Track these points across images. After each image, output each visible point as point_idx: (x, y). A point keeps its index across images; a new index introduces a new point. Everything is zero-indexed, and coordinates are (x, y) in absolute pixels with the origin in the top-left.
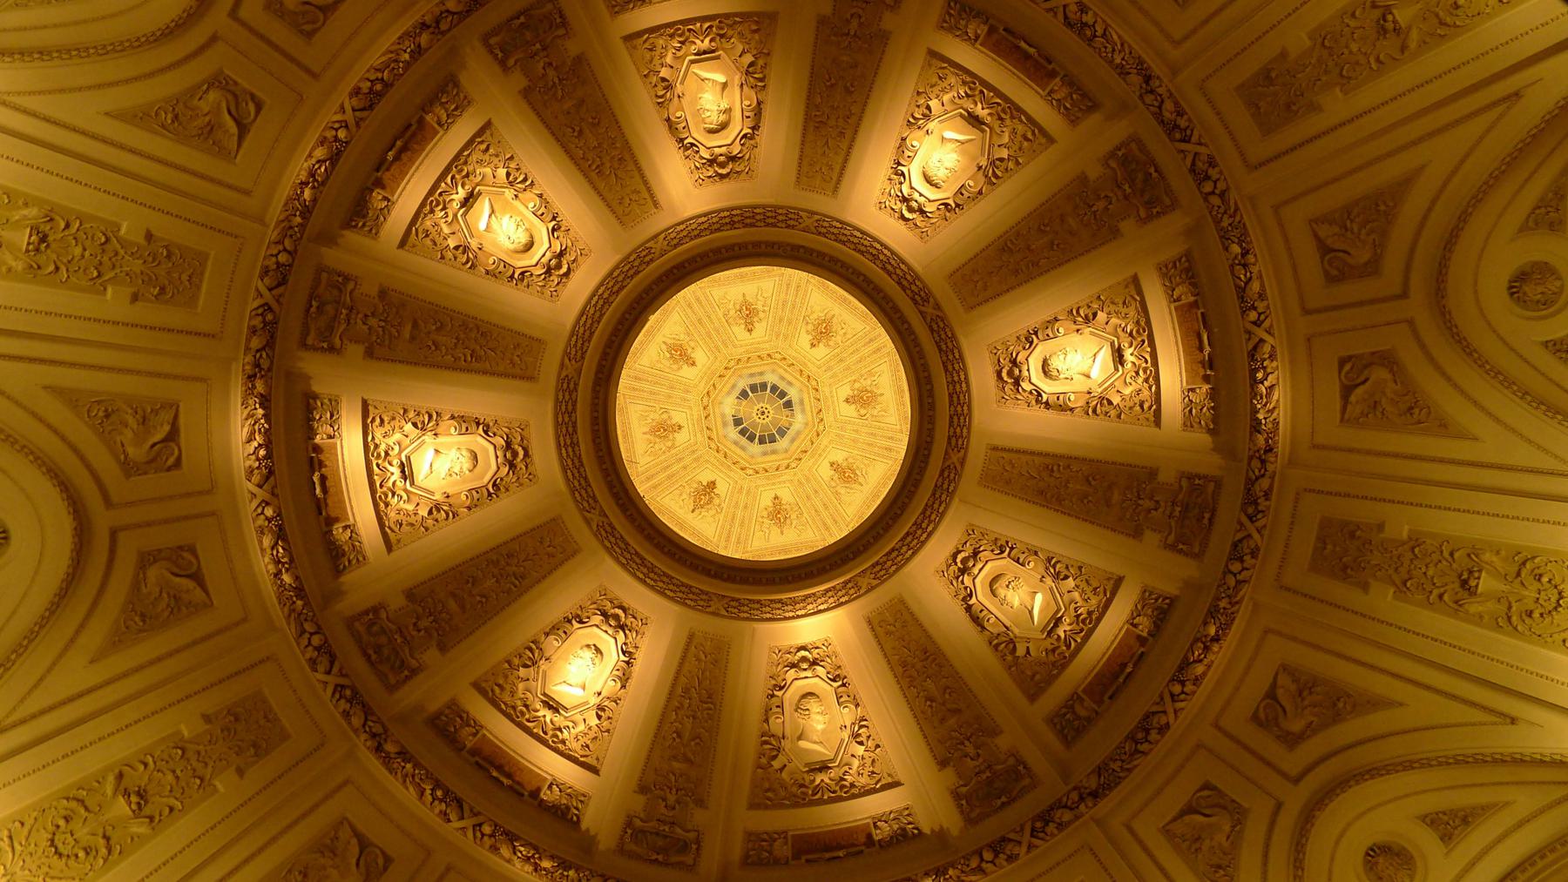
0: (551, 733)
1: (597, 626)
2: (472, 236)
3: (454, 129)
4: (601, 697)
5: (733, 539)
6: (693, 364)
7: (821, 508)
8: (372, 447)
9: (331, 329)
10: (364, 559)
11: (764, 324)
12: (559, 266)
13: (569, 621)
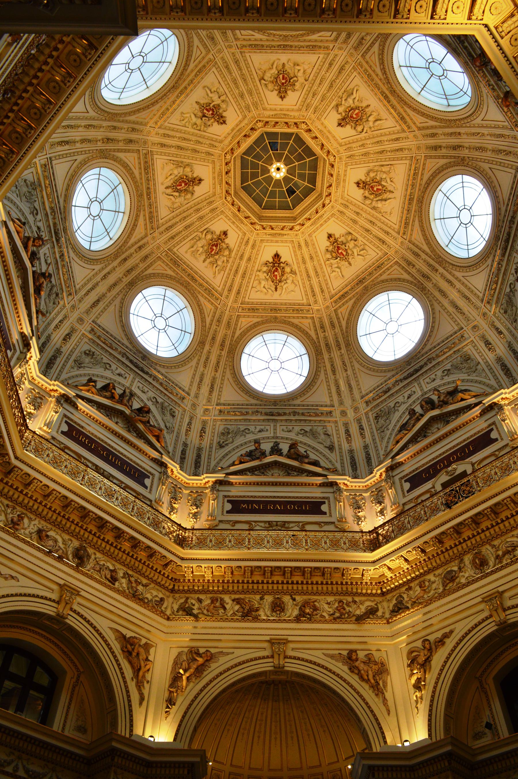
5: (317, 290)
6: (200, 180)
7: (369, 226)
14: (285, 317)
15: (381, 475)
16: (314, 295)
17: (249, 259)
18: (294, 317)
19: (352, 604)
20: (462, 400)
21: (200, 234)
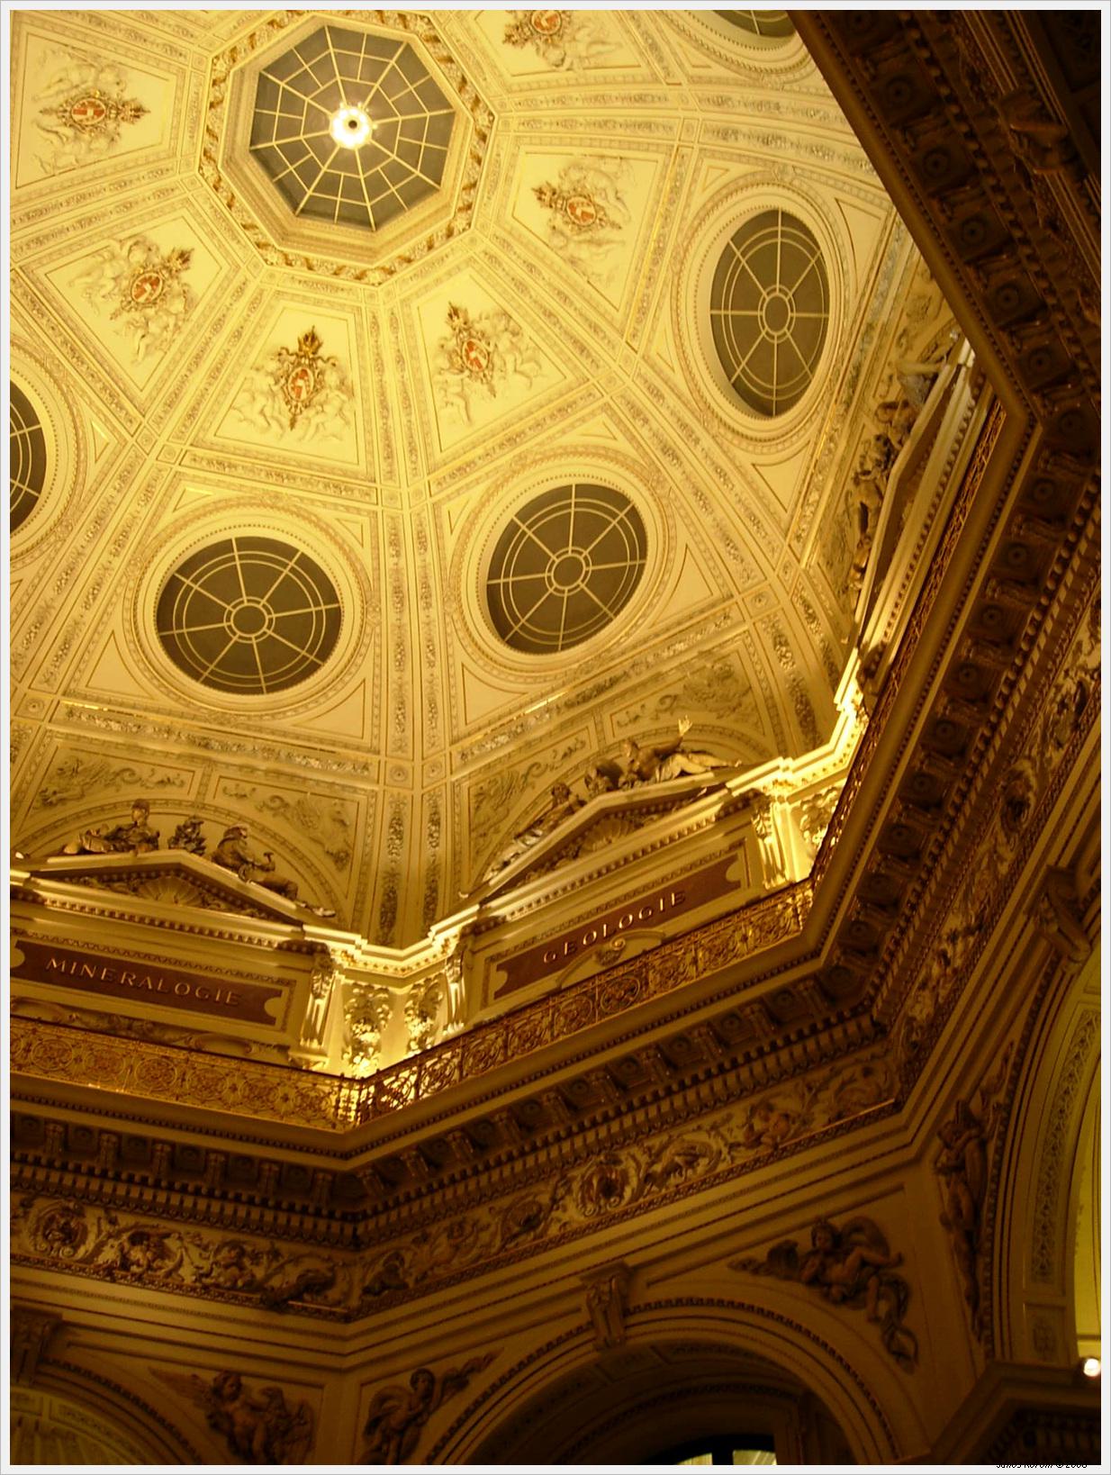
5: (399, 444)
6: (138, 112)
7: (554, 305)
14: (301, 499)
15: (445, 946)
16: (389, 456)
17: (238, 334)
18: (324, 504)
19: (265, 1260)
20: (683, 774)
21: (117, 246)
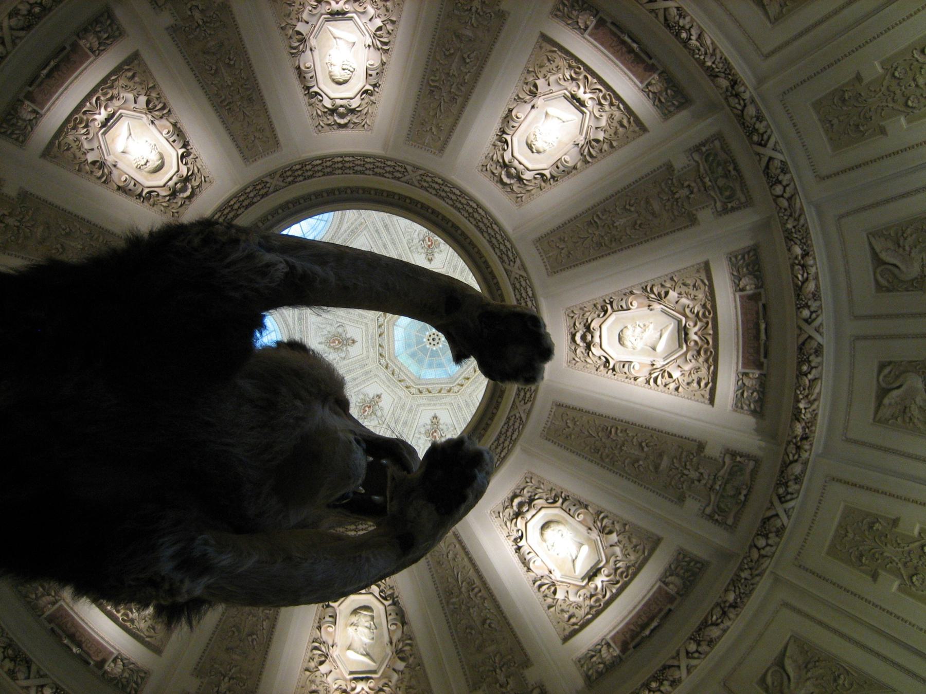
0: (581, 77)
1: (528, 169)
2: (595, 542)
3: (596, 639)
4: (532, 103)
8: (711, 360)
9: (732, 473)
10: (730, 258)
11: (422, 422)
12: (521, 505)
13: (553, 177)
